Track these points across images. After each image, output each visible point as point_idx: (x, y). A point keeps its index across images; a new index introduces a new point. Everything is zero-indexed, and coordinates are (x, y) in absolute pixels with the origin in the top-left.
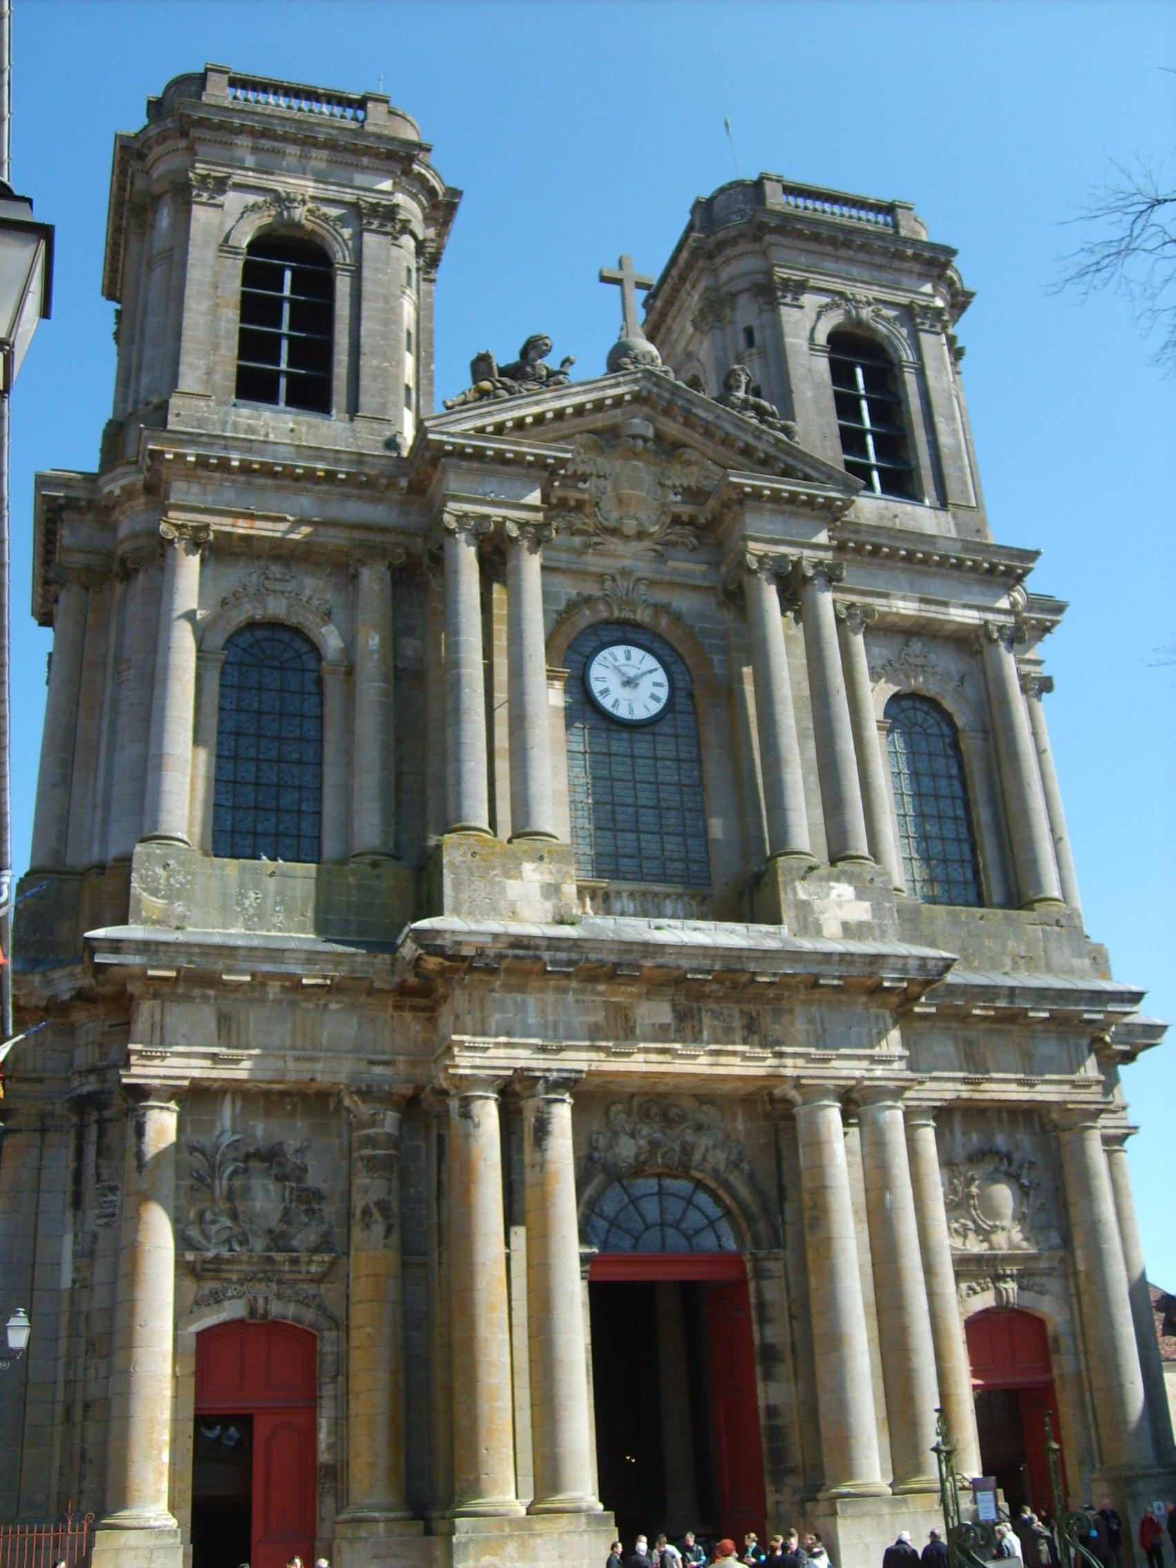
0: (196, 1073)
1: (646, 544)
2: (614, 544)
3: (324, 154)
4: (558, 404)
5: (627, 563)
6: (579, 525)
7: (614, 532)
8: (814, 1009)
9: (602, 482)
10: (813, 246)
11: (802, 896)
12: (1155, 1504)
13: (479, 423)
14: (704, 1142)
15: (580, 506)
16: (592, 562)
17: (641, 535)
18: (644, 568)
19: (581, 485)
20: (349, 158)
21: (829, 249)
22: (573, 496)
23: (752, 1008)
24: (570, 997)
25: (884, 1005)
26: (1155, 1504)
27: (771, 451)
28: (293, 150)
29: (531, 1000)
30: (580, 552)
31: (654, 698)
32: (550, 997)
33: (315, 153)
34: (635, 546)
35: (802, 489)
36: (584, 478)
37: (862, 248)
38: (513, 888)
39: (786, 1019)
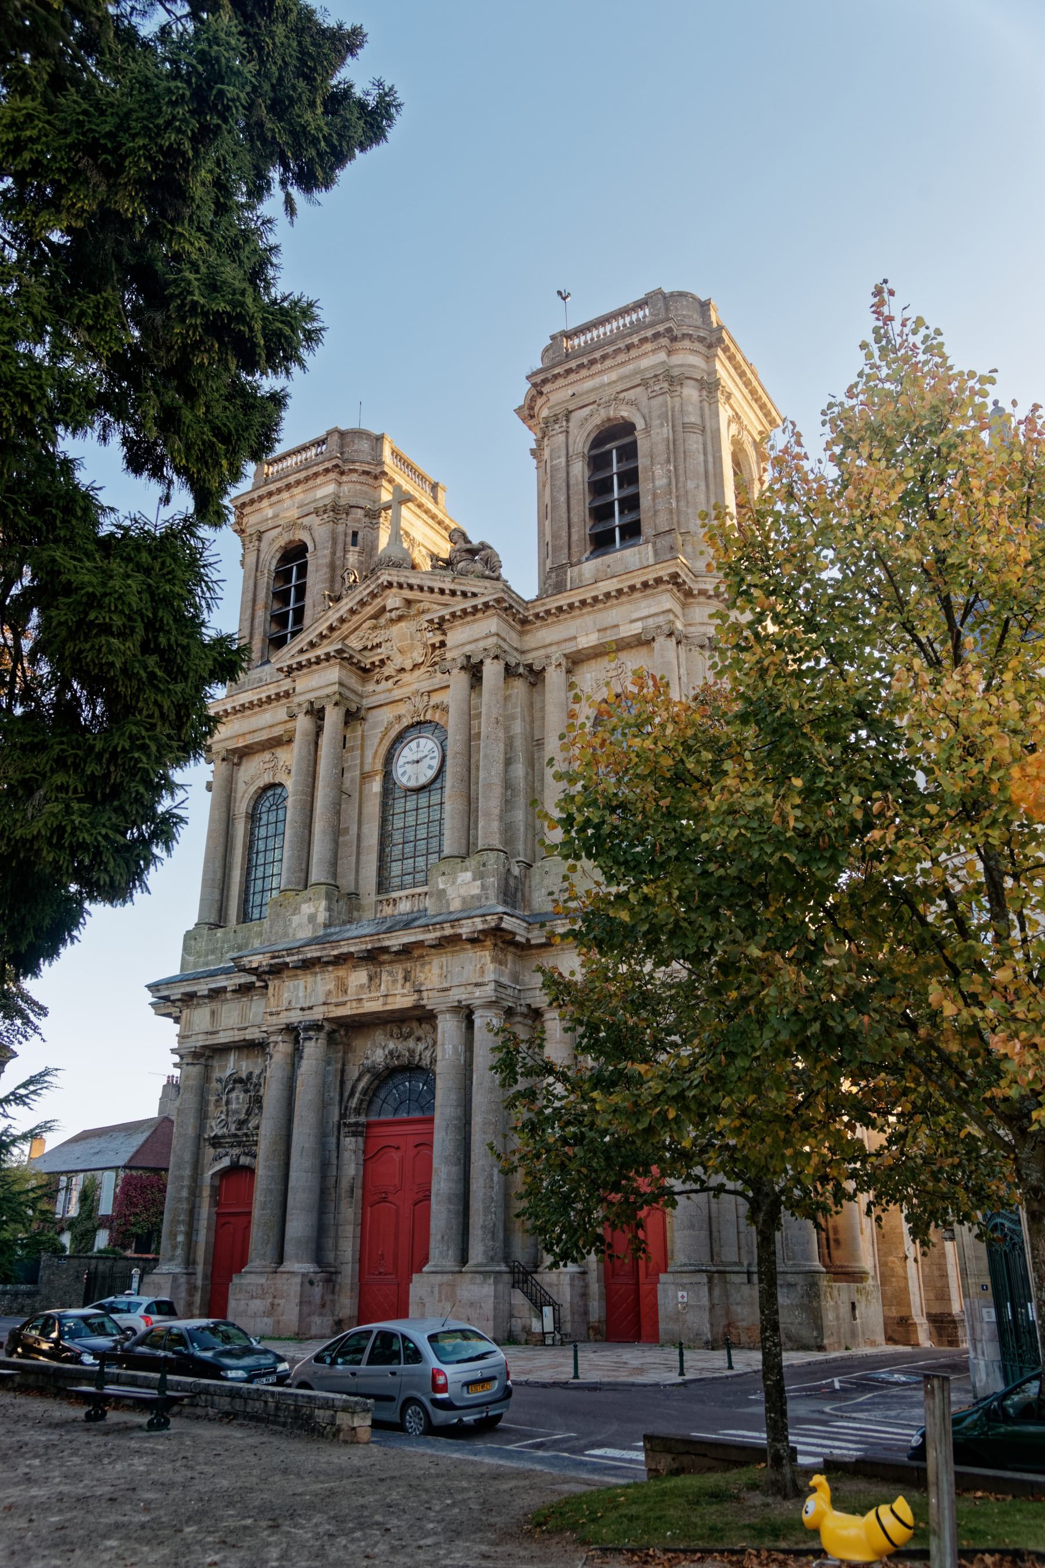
0: (201, 1044)
1: (423, 669)
2: (406, 677)
3: (300, 489)
4: (337, 615)
5: (414, 687)
6: (387, 674)
7: (402, 670)
8: (444, 959)
9: (389, 644)
10: (573, 377)
11: (441, 886)
12: (680, 1294)
13: (298, 648)
14: (420, 1047)
15: (382, 661)
16: (397, 694)
17: (416, 666)
18: (426, 686)
19: (379, 650)
20: (311, 483)
21: (584, 372)
22: (376, 659)
23: (408, 965)
24: (319, 977)
25: (484, 948)
26: (680, 1294)
27: (452, 587)
28: (285, 495)
29: (302, 983)
30: (390, 690)
31: (430, 767)
32: (310, 979)
33: (296, 491)
34: (417, 673)
35: (468, 604)
36: (379, 645)
37: (604, 357)
38: (296, 920)
39: (427, 967)
